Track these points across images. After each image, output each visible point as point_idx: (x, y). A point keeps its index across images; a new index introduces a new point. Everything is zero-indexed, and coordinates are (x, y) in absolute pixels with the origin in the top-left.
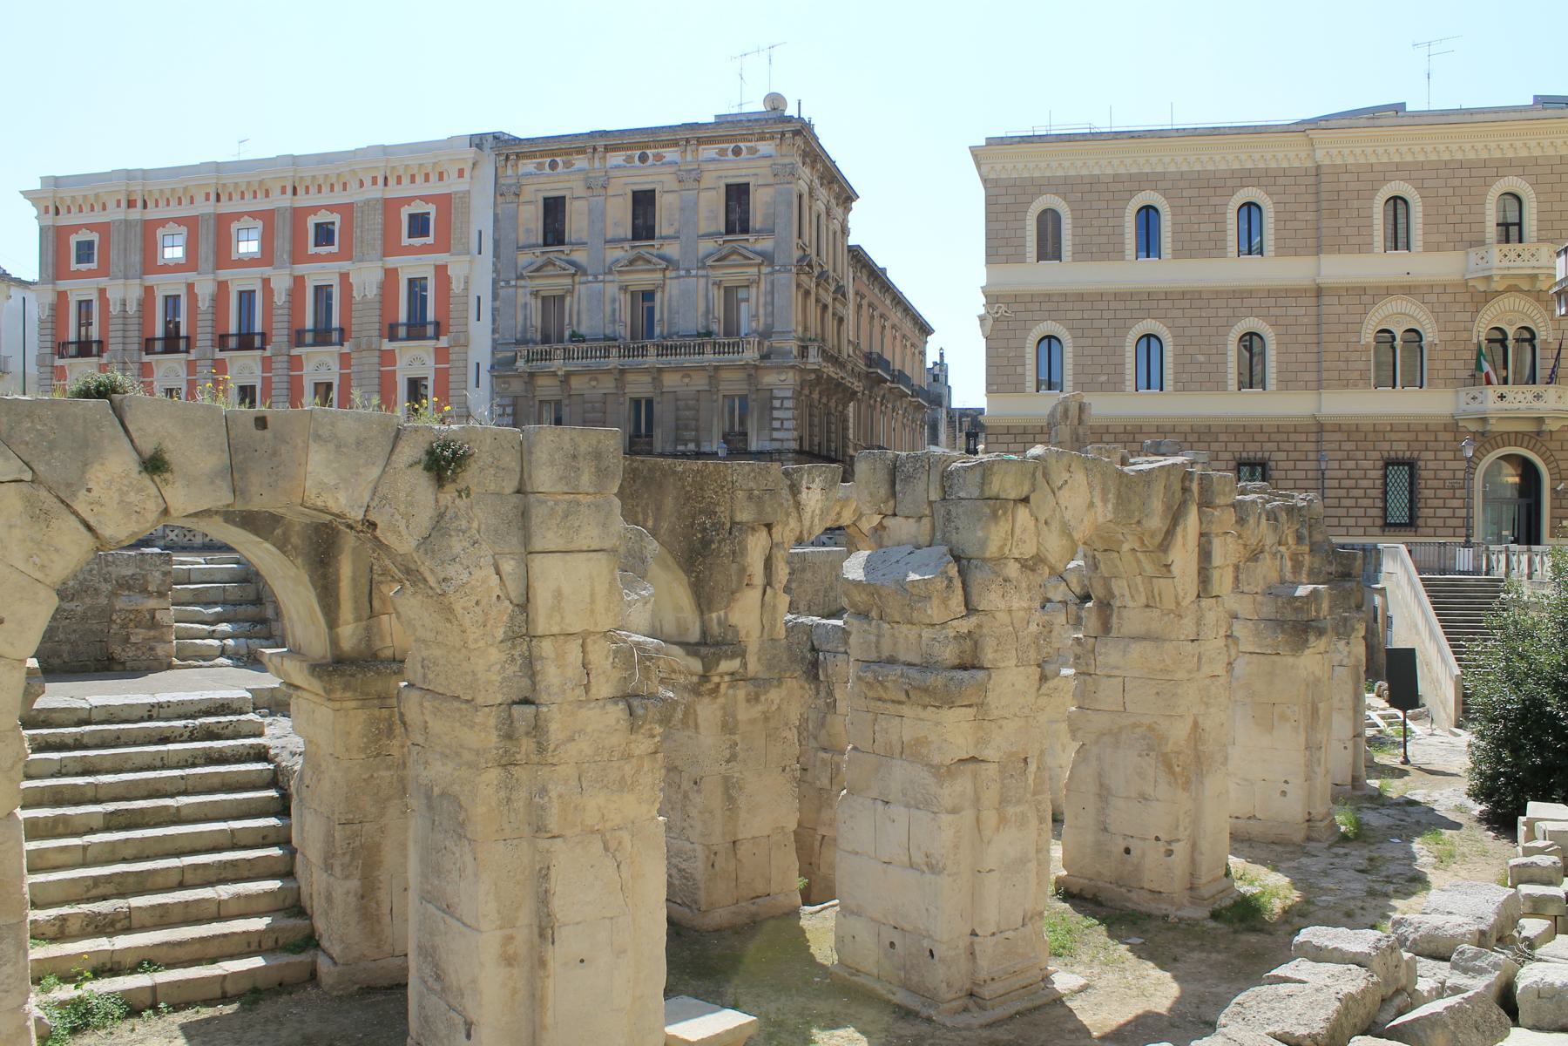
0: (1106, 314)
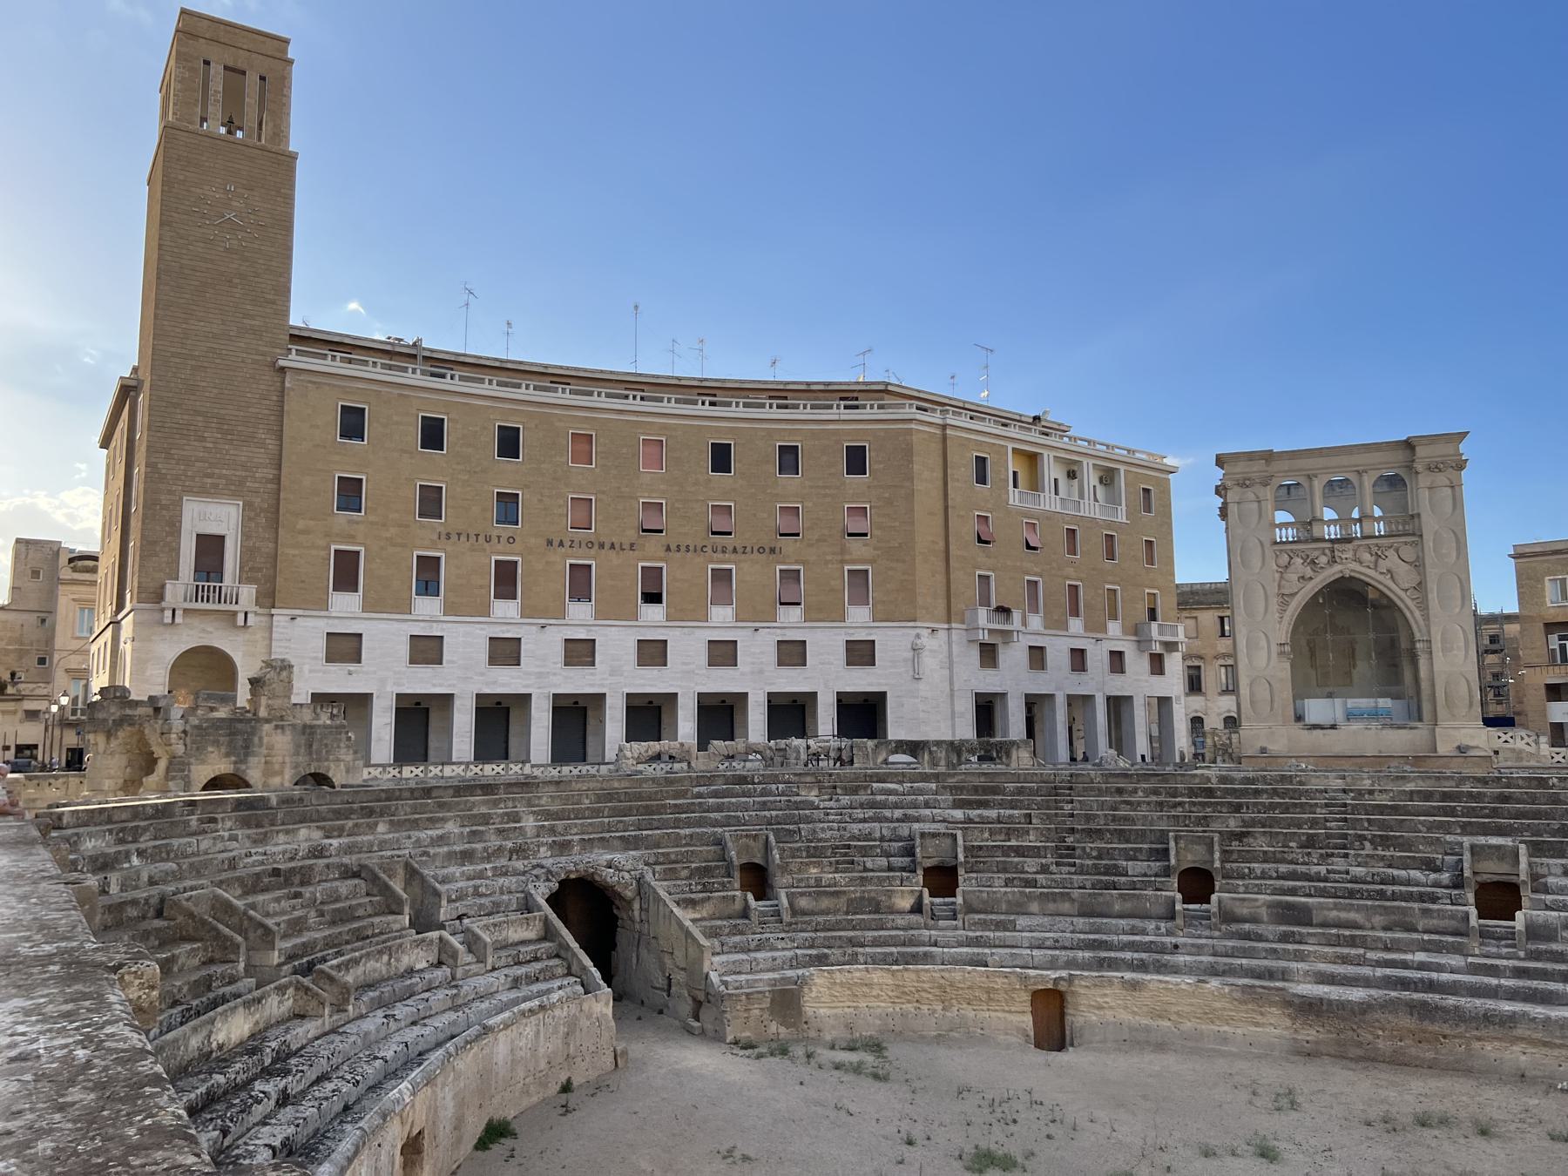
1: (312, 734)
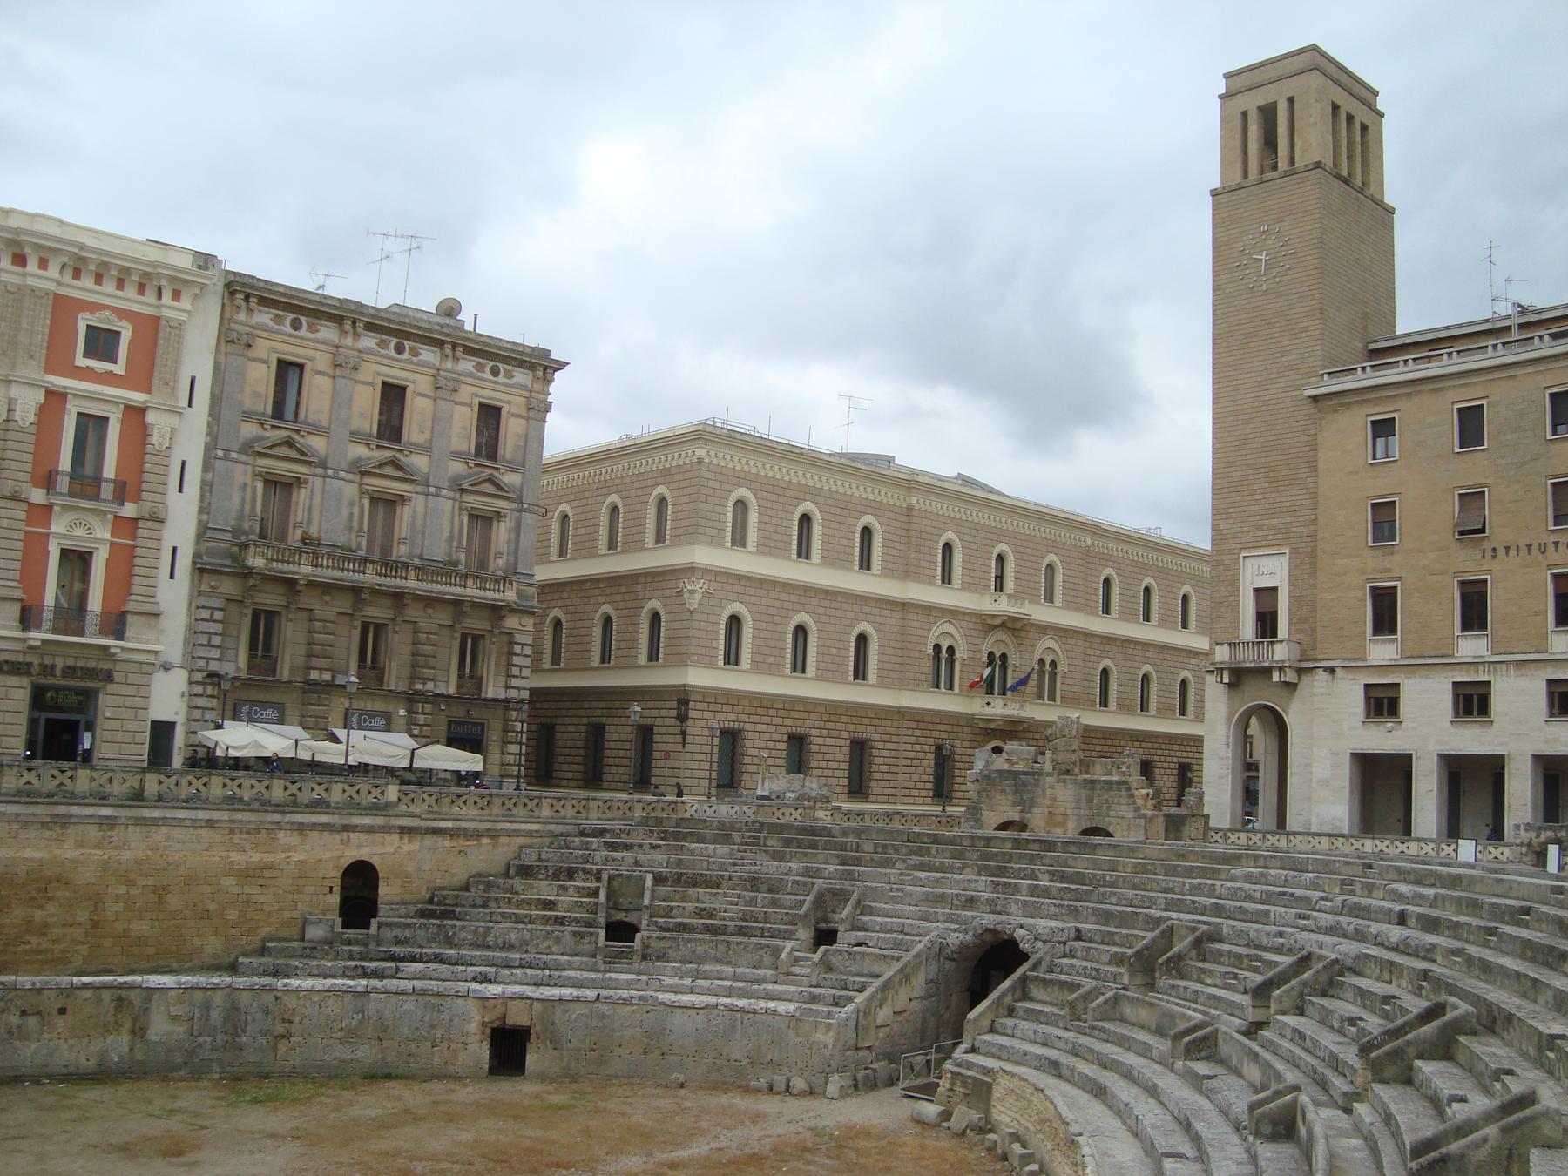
0: (777, 604)
1: (1093, 788)
